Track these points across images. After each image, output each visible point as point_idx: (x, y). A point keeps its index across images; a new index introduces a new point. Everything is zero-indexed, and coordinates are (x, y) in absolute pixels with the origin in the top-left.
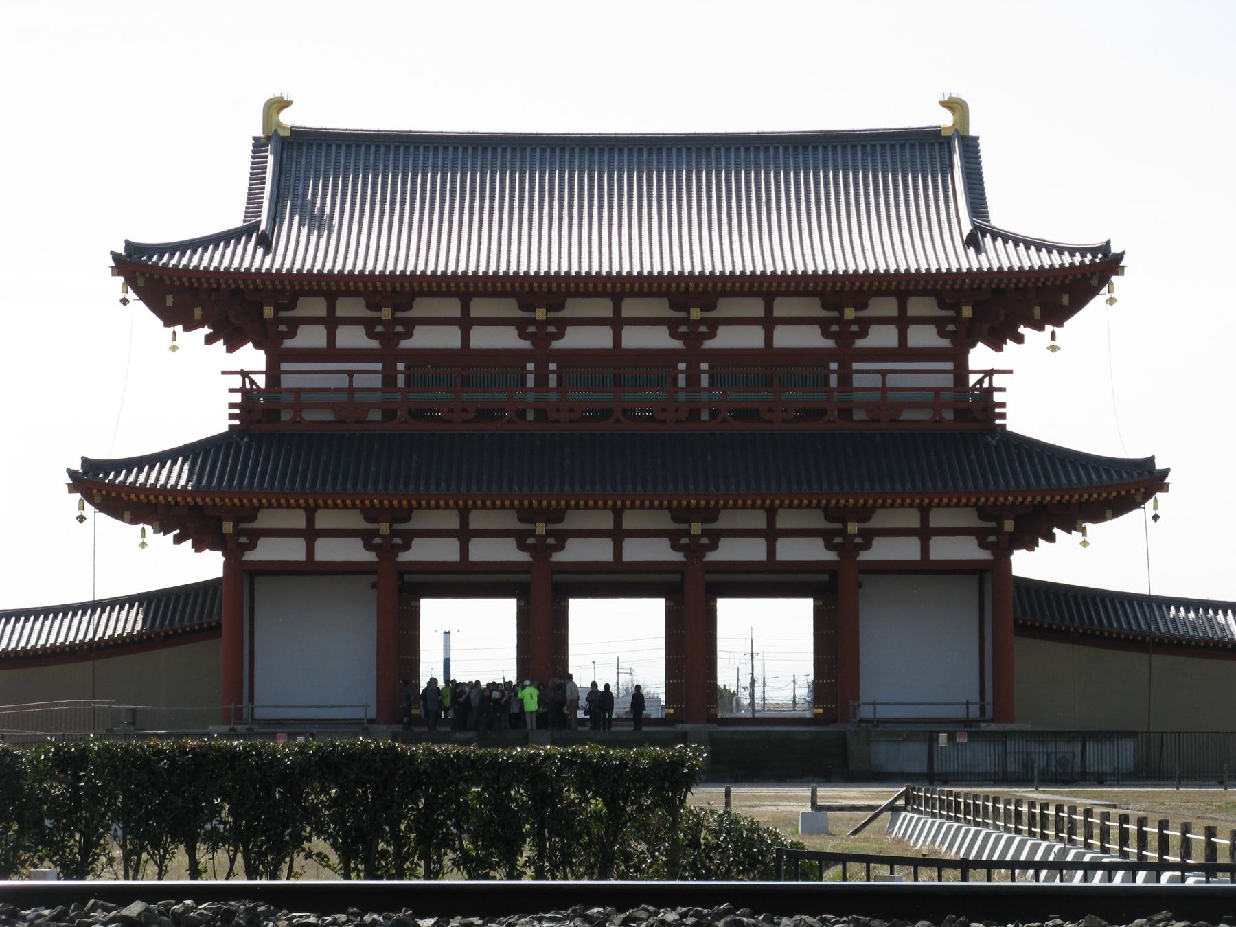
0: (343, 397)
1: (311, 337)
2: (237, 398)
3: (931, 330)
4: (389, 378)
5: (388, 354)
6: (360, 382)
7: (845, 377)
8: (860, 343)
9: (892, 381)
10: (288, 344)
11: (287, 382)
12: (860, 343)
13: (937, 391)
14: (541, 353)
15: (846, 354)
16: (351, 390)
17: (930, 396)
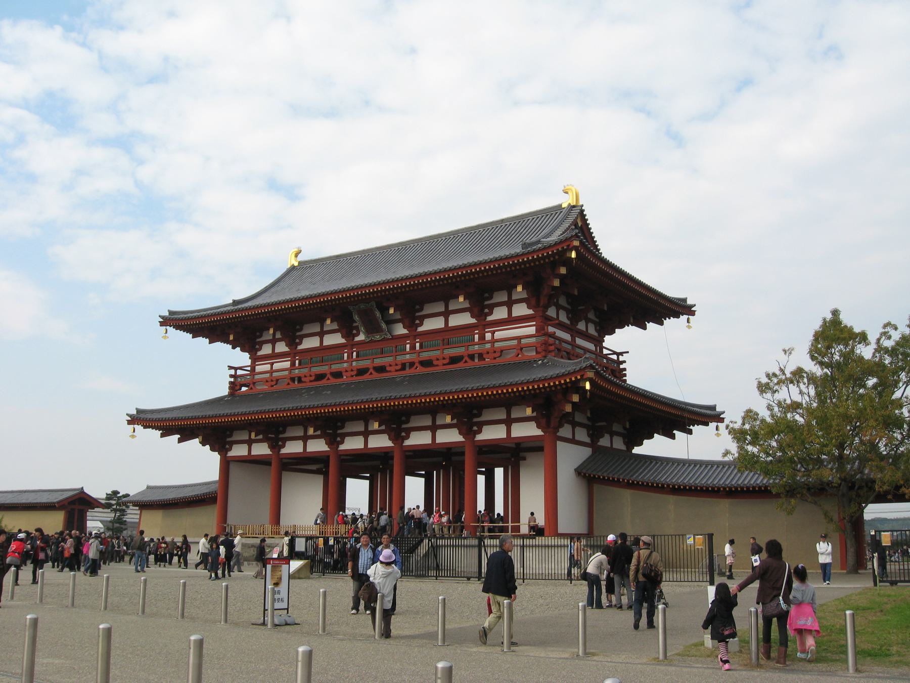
0: (268, 375)
1: (266, 350)
2: (232, 380)
3: (524, 305)
4: (293, 364)
5: (292, 354)
6: (277, 366)
7: (482, 337)
8: (489, 318)
9: (498, 335)
10: (259, 353)
11: (258, 369)
12: (489, 318)
13: (519, 338)
14: (350, 344)
15: (483, 324)
16: (272, 371)
17: (515, 342)
